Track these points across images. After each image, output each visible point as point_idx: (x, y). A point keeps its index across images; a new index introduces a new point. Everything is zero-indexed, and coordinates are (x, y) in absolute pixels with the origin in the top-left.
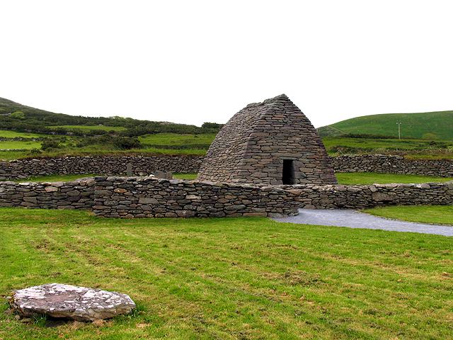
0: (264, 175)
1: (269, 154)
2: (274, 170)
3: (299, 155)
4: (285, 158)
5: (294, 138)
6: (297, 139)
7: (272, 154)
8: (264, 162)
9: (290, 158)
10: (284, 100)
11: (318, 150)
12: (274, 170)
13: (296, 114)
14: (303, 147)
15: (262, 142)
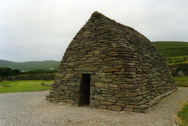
0: (66, 88)
1: (72, 69)
2: (74, 84)
3: (95, 69)
4: (83, 72)
5: (92, 52)
6: (97, 52)
7: (74, 70)
8: (68, 76)
9: (86, 73)
10: (97, 17)
11: (117, 62)
12: (74, 84)
13: (102, 27)
14: (101, 60)
15: (68, 59)
